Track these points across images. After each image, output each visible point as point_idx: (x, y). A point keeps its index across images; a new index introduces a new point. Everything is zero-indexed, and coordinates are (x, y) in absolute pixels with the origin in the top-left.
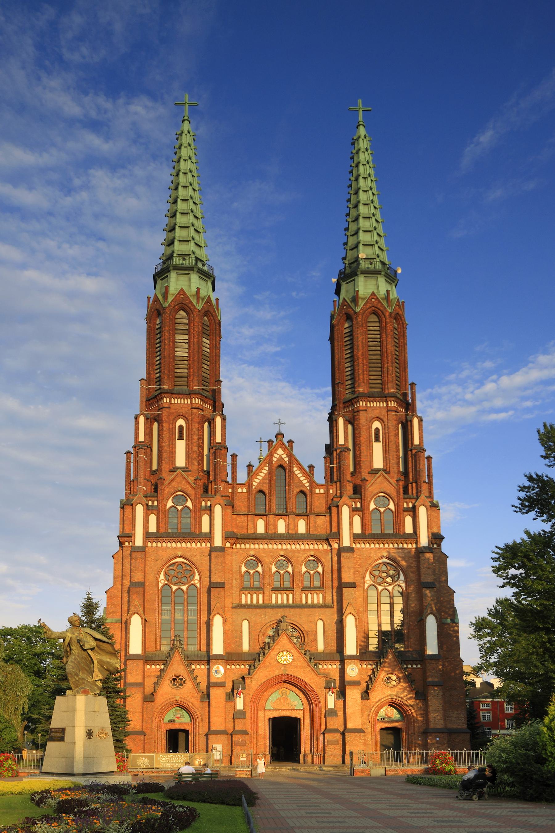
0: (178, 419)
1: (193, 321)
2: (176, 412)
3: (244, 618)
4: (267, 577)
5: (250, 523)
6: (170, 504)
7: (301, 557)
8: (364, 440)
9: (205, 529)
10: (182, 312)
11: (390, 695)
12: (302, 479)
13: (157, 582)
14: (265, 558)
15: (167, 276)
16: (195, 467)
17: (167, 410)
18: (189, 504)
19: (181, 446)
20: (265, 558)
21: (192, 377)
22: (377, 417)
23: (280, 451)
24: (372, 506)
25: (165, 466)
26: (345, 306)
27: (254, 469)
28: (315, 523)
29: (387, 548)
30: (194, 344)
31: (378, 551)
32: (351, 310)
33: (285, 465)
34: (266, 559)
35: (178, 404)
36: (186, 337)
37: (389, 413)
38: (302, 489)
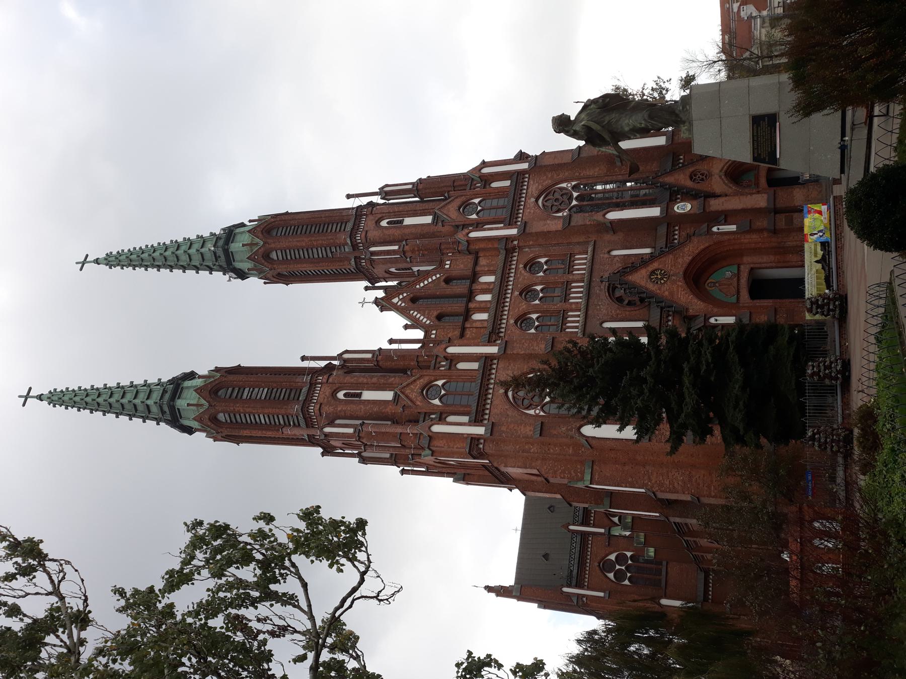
0: (336, 397)
1: (231, 381)
2: (328, 398)
3: (598, 326)
4: (545, 307)
5: (474, 325)
6: (436, 402)
7: (525, 276)
8: (398, 232)
9: (475, 366)
10: (220, 393)
11: (720, 177)
12: (430, 280)
13: (537, 415)
14: (521, 309)
15: (178, 409)
16: (394, 379)
17: (323, 406)
18: (440, 383)
19: (368, 395)
20: (521, 309)
21: (292, 384)
22: (376, 222)
23: (395, 300)
24: (474, 216)
25: (389, 409)
26: (254, 257)
27: (409, 323)
28: (484, 266)
29: (525, 199)
30: (257, 381)
31: (528, 206)
32: (260, 250)
33: (412, 295)
34: (523, 306)
35: (318, 397)
36: (247, 390)
37: (373, 213)
38: (442, 280)
